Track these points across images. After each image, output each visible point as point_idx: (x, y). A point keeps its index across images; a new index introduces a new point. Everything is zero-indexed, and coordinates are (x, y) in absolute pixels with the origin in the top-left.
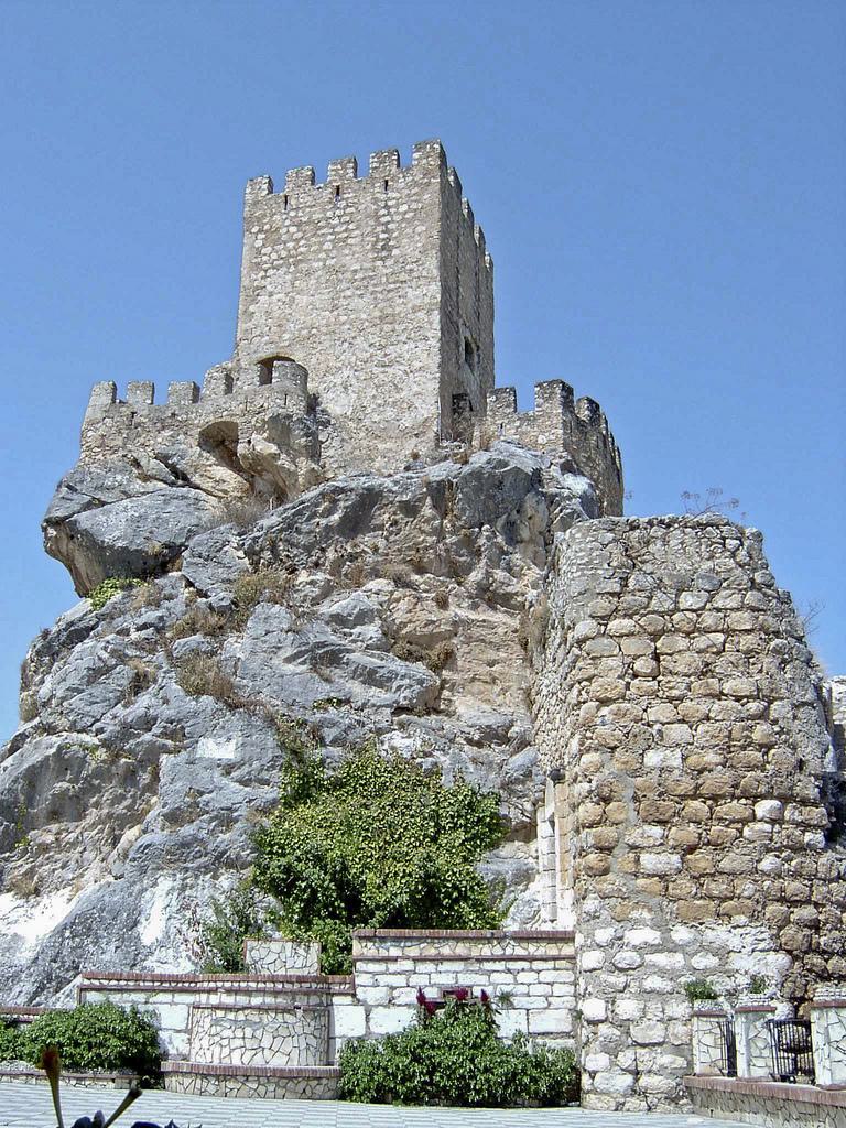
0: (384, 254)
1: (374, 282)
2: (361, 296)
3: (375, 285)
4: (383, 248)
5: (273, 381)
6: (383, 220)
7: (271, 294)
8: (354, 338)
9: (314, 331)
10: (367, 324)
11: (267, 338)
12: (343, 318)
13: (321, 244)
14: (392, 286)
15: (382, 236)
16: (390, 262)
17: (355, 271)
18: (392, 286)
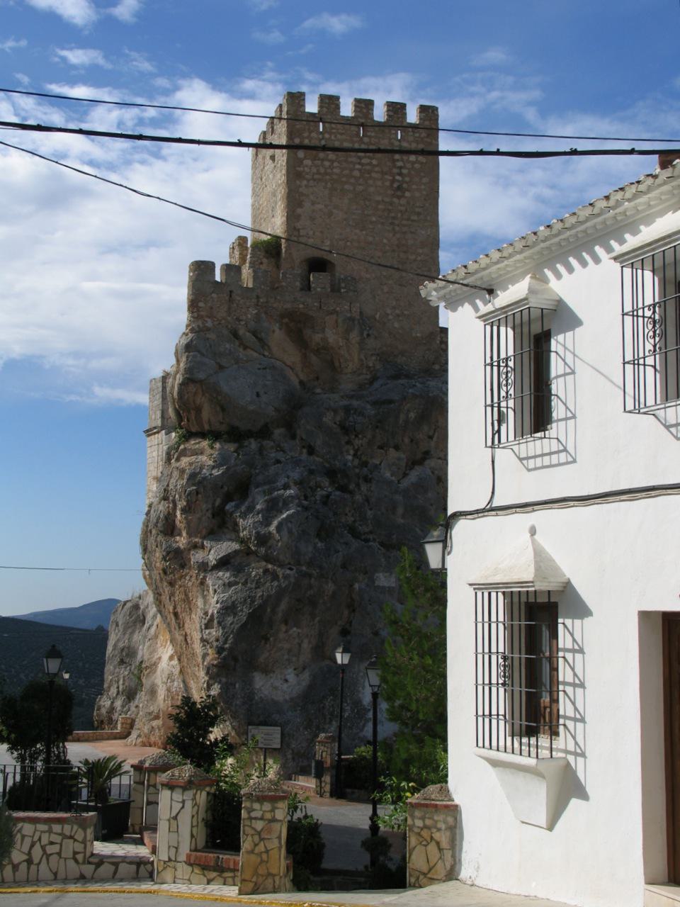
0: (399, 193)
1: (393, 215)
2: (383, 224)
3: (394, 218)
4: (399, 188)
5: (342, 290)
6: (400, 164)
7: (313, 204)
8: (379, 257)
9: (349, 244)
10: (387, 248)
11: (312, 240)
12: (370, 239)
13: (352, 170)
14: (404, 222)
15: (398, 178)
16: (403, 201)
17: (378, 202)
18: (404, 222)
